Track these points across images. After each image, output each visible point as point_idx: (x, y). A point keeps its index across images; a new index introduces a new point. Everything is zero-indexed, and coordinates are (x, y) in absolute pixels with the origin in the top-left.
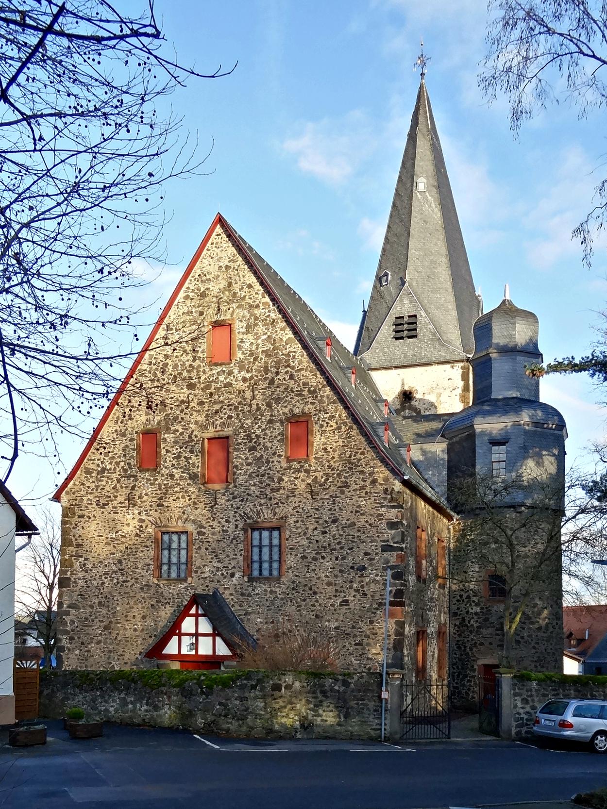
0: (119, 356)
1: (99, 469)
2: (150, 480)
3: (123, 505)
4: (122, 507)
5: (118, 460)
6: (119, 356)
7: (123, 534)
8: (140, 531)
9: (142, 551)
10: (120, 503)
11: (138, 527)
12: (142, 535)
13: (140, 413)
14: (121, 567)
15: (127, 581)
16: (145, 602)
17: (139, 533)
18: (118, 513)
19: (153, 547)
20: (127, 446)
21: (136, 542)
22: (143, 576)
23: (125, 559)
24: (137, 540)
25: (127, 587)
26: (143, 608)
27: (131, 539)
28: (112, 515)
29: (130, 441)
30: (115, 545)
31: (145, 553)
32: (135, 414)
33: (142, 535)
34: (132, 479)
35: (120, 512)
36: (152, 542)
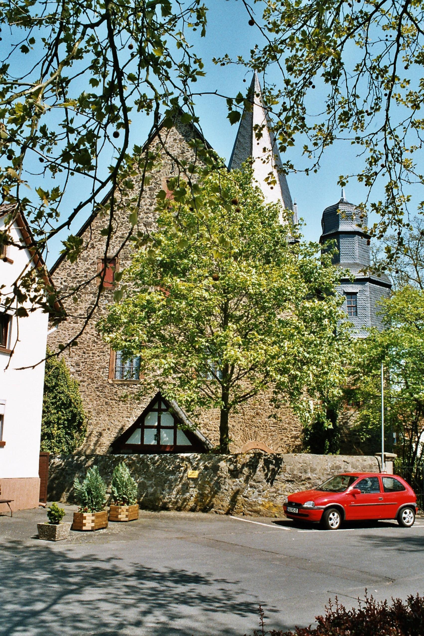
0: (45, 9)
1: (62, 286)
2: (108, 297)
3: (83, 317)
4: (81, 318)
5: (80, 280)
6: (45, 9)
7: (82, 341)
8: (97, 339)
9: (98, 356)
10: (80, 315)
11: (95, 335)
12: (99, 343)
13: (102, 243)
14: (78, 369)
15: (84, 382)
16: (100, 399)
17: (96, 340)
18: (77, 323)
19: (109, 352)
20: (89, 269)
21: (93, 348)
22: (98, 377)
23: (83, 362)
24: (94, 346)
25: (83, 386)
26: (98, 405)
27: (88, 346)
28: (72, 325)
29: (91, 264)
30: (74, 350)
31: (102, 357)
32: (97, 244)
33: (99, 343)
34: (92, 295)
35: (79, 322)
36: (108, 349)
